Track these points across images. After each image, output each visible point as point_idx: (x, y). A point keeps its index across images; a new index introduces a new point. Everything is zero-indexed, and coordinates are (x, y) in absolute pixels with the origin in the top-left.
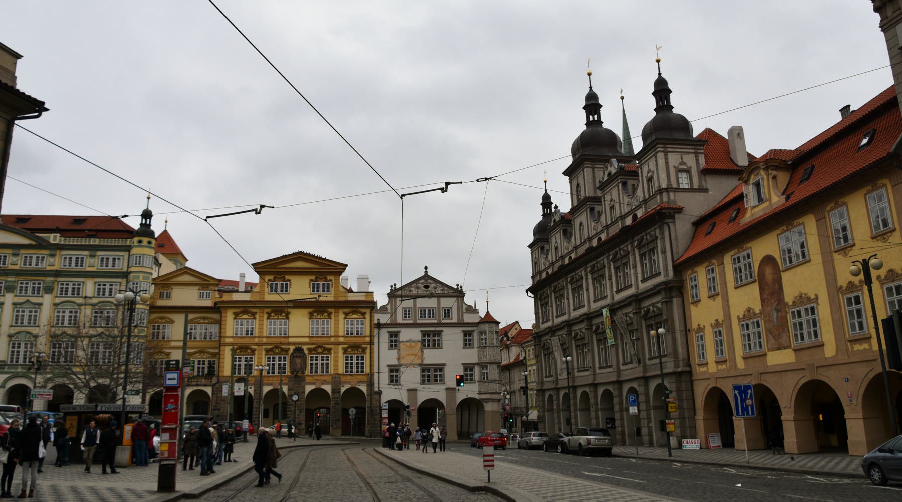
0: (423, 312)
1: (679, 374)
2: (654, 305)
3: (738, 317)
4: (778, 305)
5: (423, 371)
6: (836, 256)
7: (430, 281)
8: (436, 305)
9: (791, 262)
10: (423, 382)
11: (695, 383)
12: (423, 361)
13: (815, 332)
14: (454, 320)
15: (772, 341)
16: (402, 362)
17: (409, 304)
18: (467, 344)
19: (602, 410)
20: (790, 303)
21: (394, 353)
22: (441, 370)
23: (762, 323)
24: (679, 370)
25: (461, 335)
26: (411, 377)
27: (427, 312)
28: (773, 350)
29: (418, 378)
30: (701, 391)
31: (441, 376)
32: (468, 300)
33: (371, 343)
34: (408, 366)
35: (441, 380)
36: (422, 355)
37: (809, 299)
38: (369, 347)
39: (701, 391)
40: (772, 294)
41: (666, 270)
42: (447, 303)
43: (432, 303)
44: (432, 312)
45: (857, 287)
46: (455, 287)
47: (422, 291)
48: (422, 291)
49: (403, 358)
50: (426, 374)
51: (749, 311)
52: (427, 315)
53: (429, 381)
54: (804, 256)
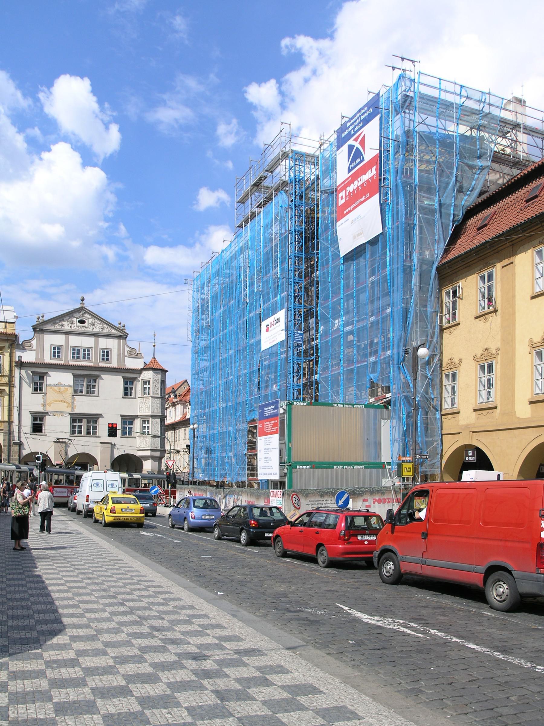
0: (76, 352)
3: (531, 340)
5: (73, 420)
7: (87, 315)
8: (93, 345)
10: (73, 433)
12: (73, 409)
14: (114, 363)
16: (48, 409)
17: (59, 340)
18: (127, 392)
21: (39, 397)
22: (95, 421)
25: (122, 380)
26: (58, 426)
27: (81, 352)
29: (68, 428)
31: (95, 428)
32: (131, 342)
33: (11, 385)
34: (55, 413)
35: (95, 433)
36: (73, 402)
38: (7, 389)
42: (104, 343)
43: (88, 342)
44: (87, 353)
46: (117, 326)
47: (76, 326)
48: (76, 326)
49: (49, 404)
50: (77, 424)
52: (81, 356)
53: (80, 432)
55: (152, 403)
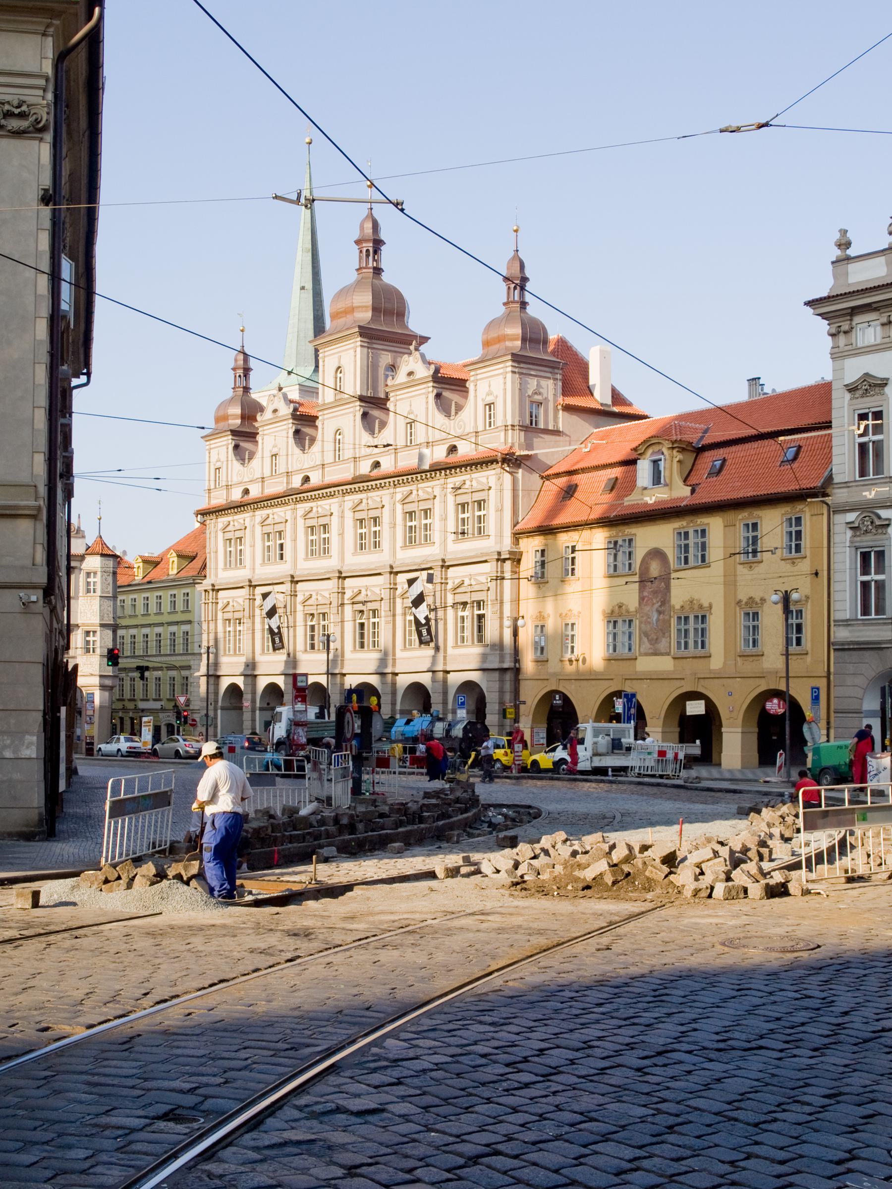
1: (503, 671)
2: (470, 577)
4: (660, 606)
6: (740, 567)
9: (686, 562)
11: (522, 683)
13: (703, 643)
15: (646, 645)
19: (223, 709)
20: (678, 607)
23: (636, 623)
24: (506, 665)
28: (646, 654)
30: (531, 694)
37: (701, 607)
39: (531, 694)
40: (655, 593)
41: (501, 535)
45: (757, 603)
51: (620, 607)
54: (703, 560)
55: (100, 606)
